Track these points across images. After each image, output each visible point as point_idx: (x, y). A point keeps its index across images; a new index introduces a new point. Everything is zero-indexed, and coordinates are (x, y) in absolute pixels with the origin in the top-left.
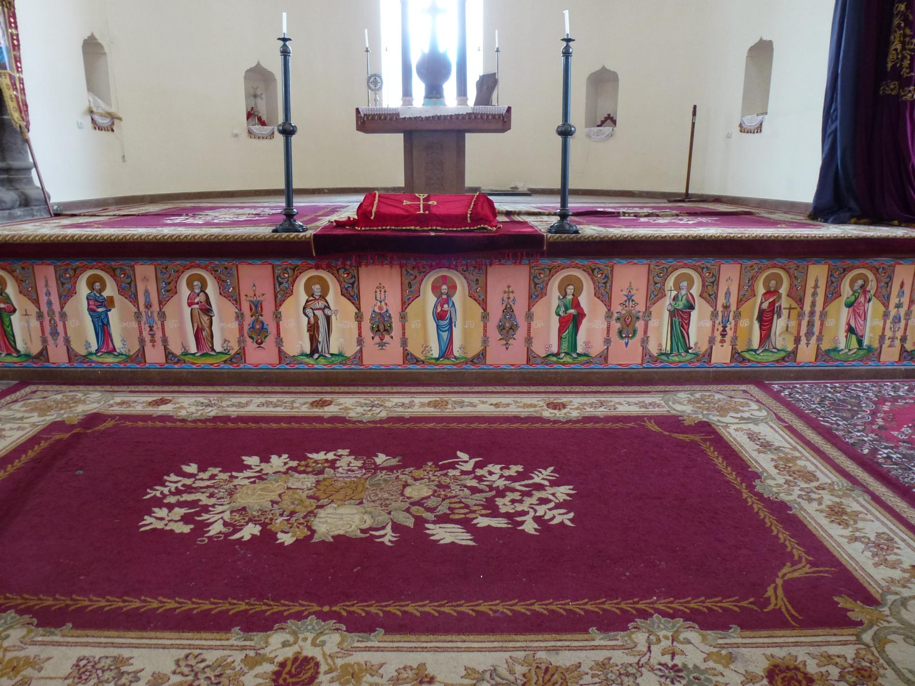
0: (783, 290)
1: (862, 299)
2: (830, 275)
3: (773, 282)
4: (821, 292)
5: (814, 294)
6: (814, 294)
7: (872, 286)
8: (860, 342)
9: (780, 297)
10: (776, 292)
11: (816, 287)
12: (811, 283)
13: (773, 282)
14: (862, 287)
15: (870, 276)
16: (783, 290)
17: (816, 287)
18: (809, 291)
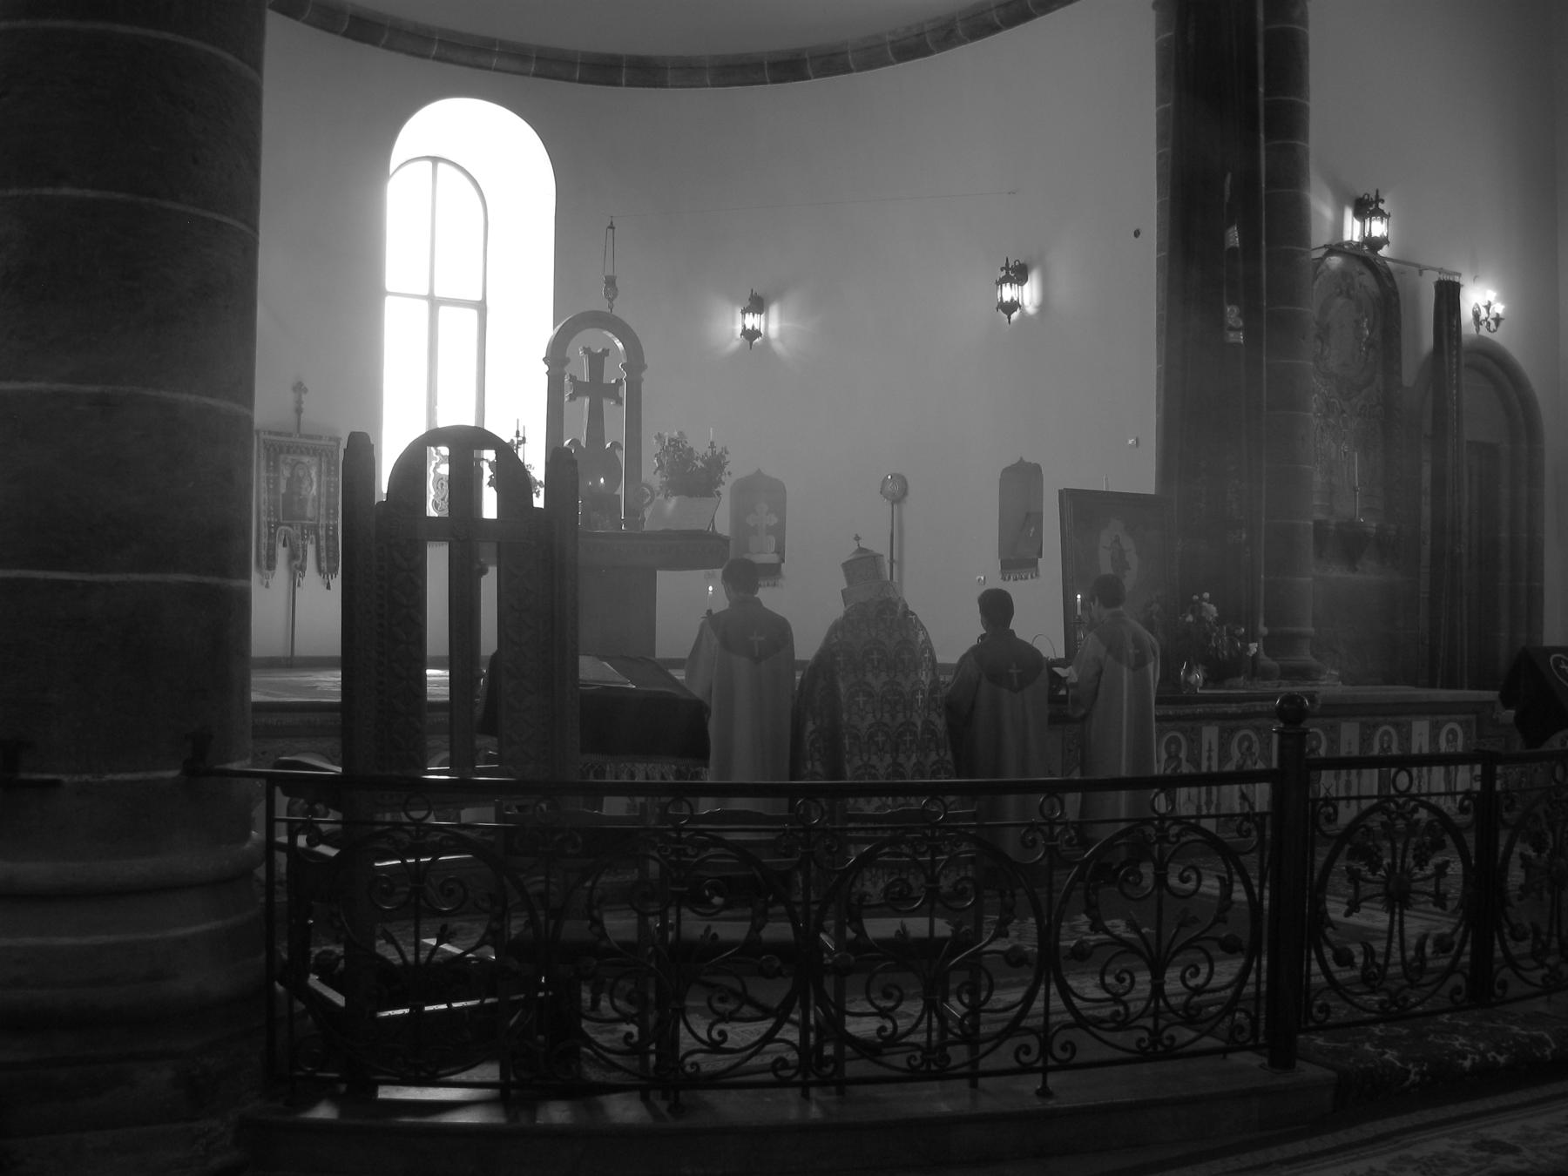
0: (1183, 755)
1: (1249, 762)
2: (1221, 737)
3: (1173, 747)
4: (1215, 755)
5: (1209, 758)
6: (1209, 758)
7: (1256, 748)
8: (1252, 807)
9: (1180, 760)
10: (1176, 757)
11: (1210, 750)
12: (1205, 747)
13: (1173, 747)
14: (1249, 748)
15: (1254, 738)
16: (1183, 755)
17: (1210, 750)
18: (1205, 755)
